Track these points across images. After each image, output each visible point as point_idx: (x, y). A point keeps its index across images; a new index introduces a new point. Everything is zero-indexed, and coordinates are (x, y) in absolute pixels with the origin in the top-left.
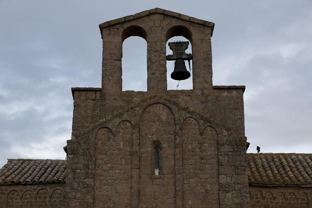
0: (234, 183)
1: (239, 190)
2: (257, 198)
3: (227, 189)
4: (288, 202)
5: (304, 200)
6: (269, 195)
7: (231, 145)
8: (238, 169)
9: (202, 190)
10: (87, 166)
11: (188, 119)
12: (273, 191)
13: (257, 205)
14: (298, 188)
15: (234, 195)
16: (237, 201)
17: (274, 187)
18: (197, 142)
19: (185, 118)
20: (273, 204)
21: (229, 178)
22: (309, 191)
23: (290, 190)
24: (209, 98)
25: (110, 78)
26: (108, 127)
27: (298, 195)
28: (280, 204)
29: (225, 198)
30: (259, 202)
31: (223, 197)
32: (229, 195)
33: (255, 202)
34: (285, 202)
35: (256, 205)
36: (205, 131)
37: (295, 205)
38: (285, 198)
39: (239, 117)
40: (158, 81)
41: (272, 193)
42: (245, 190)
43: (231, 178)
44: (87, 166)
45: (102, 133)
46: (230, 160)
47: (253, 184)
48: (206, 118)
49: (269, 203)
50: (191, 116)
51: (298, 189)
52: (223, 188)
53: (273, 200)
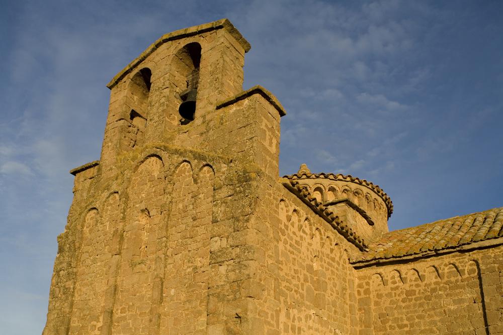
0: (231, 246)
1: (238, 256)
2: (394, 283)
3: (219, 260)
4: (446, 279)
5: (474, 273)
6: (413, 274)
7: (232, 185)
8: (238, 221)
9: (189, 270)
10: (70, 265)
11: (182, 164)
12: (418, 265)
13: (395, 293)
14: (458, 253)
15: (230, 268)
16: (232, 276)
17: (415, 260)
18: (190, 195)
19: (176, 165)
20: (420, 288)
21: (224, 240)
22: (481, 255)
23: (447, 259)
24: (211, 124)
25: (110, 144)
26: (95, 207)
27: (462, 264)
28: (433, 286)
29: (216, 275)
30: (397, 288)
31: (213, 274)
32: (223, 269)
33: (392, 289)
34: (440, 280)
35: (393, 295)
36: (201, 175)
37: (459, 283)
38: (439, 275)
39: (250, 136)
40: (155, 127)
41: (417, 271)
42: (246, 254)
43: (227, 238)
44: (70, 265)
45: (91, 217)
46: (228, 209)
47: (381, 261)
48: (199, 155)
49: (414, 288)
50: (184, 159)
51: (460, 256)
52: (215, 259)
53: (419, 282)
